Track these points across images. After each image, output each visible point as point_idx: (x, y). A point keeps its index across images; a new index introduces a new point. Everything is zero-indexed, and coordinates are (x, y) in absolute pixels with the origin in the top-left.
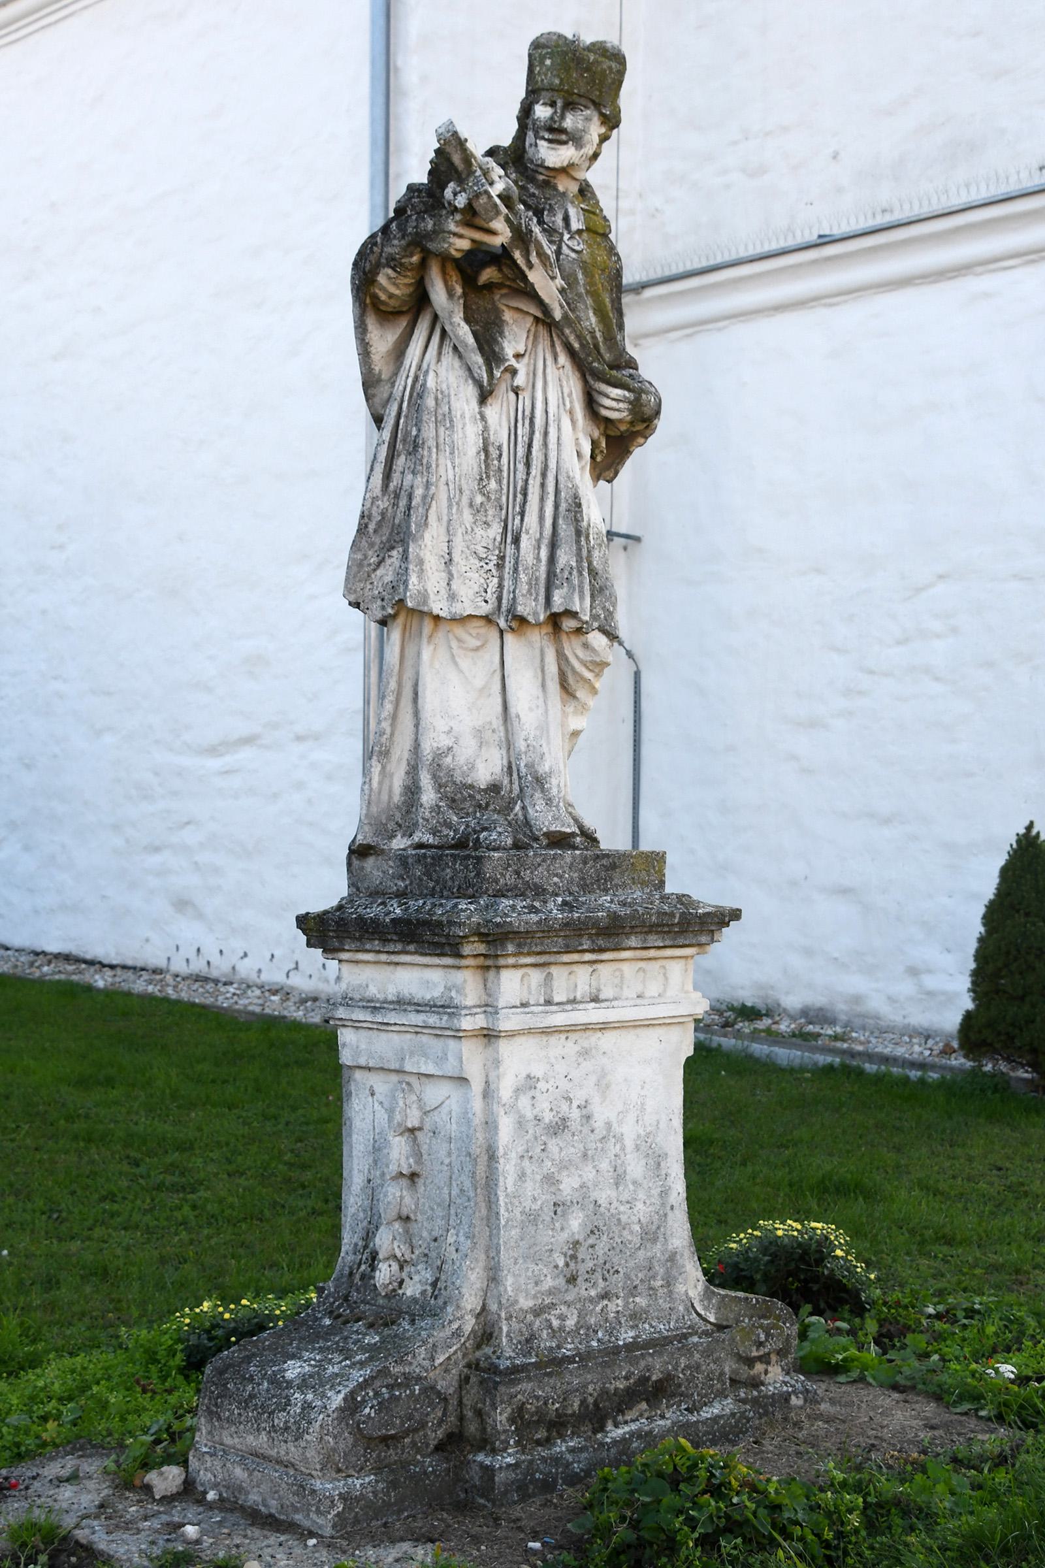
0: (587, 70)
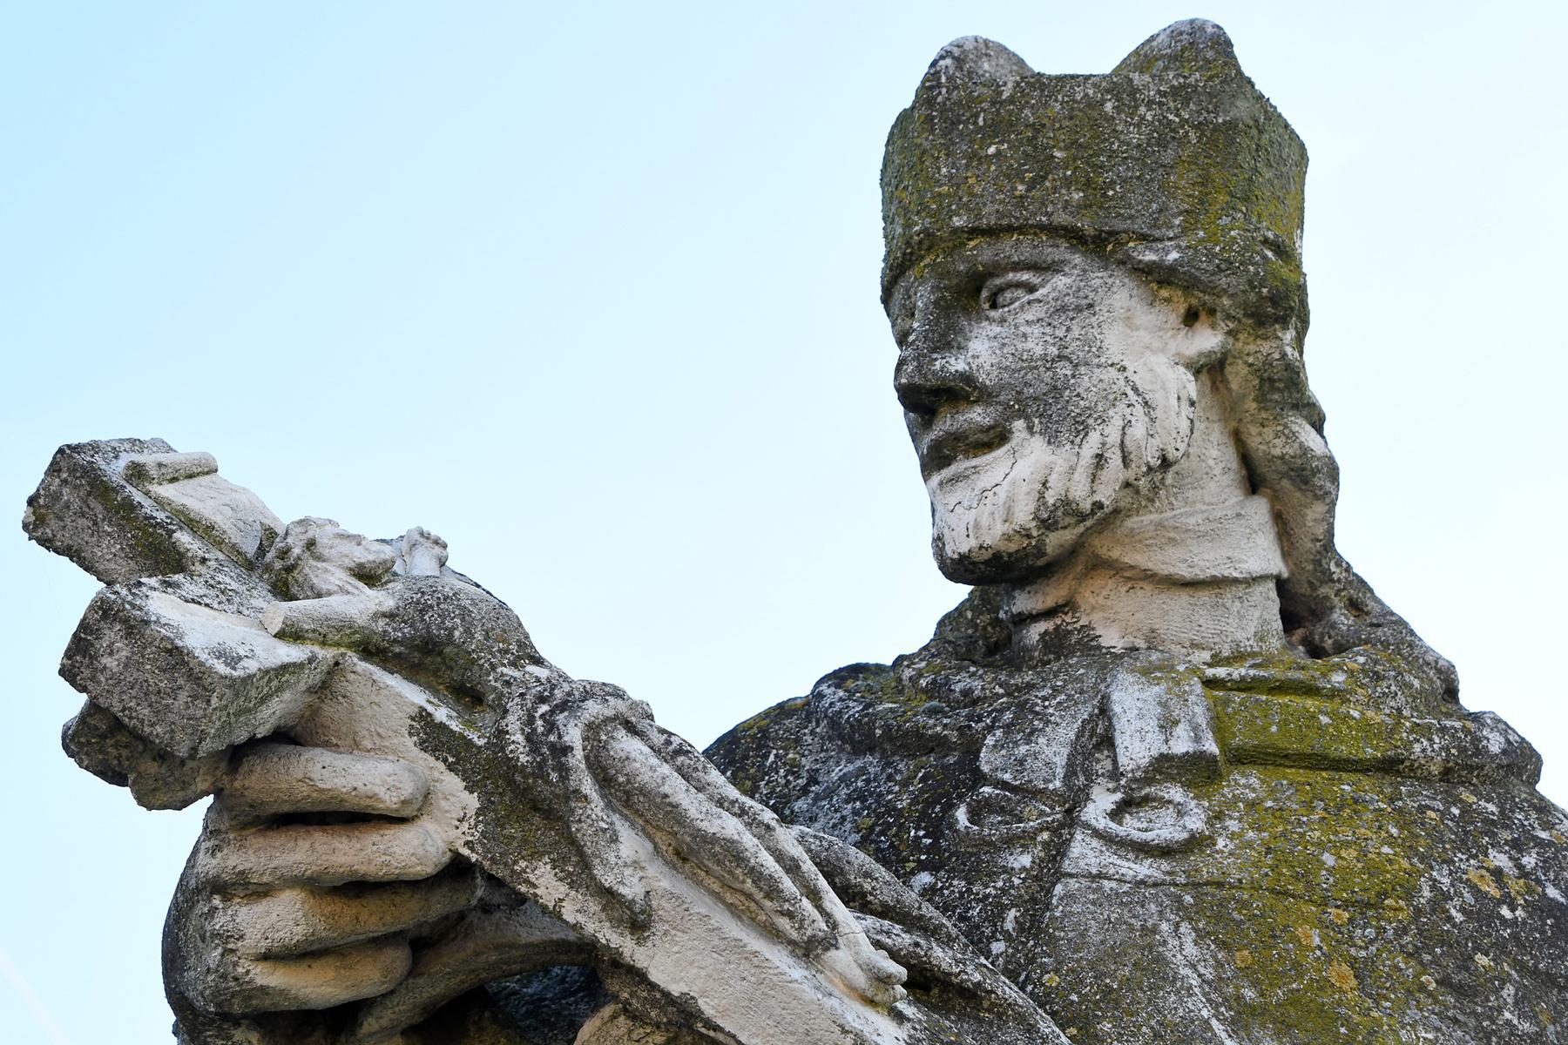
0: (995, 130)
